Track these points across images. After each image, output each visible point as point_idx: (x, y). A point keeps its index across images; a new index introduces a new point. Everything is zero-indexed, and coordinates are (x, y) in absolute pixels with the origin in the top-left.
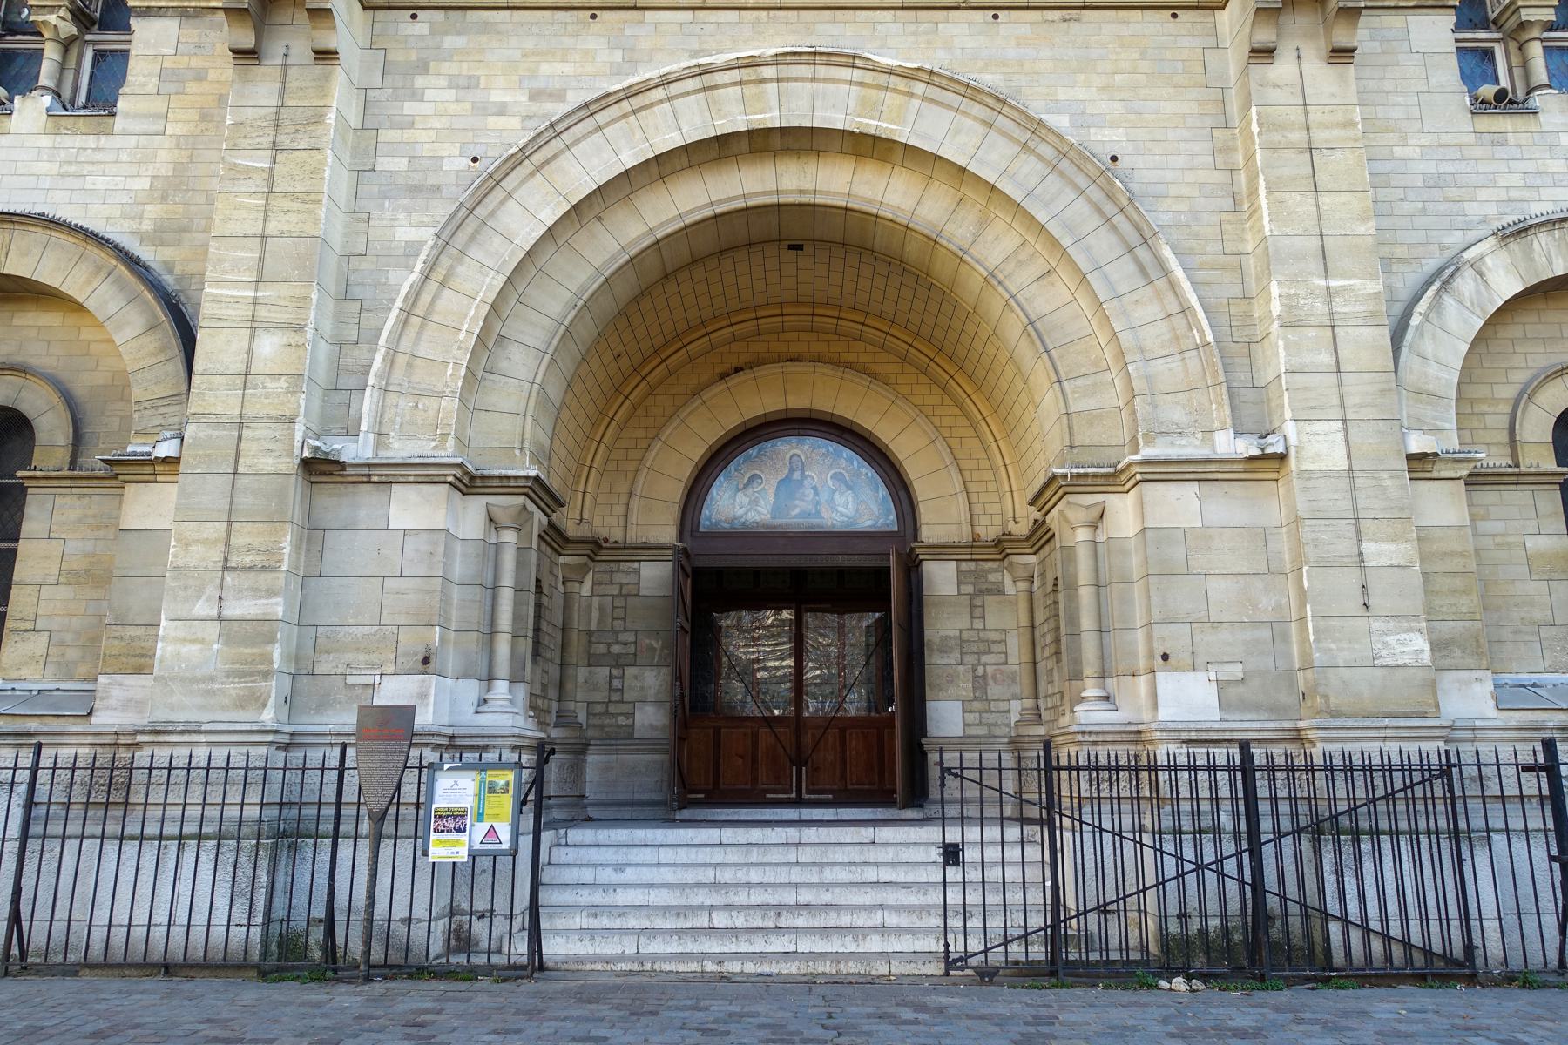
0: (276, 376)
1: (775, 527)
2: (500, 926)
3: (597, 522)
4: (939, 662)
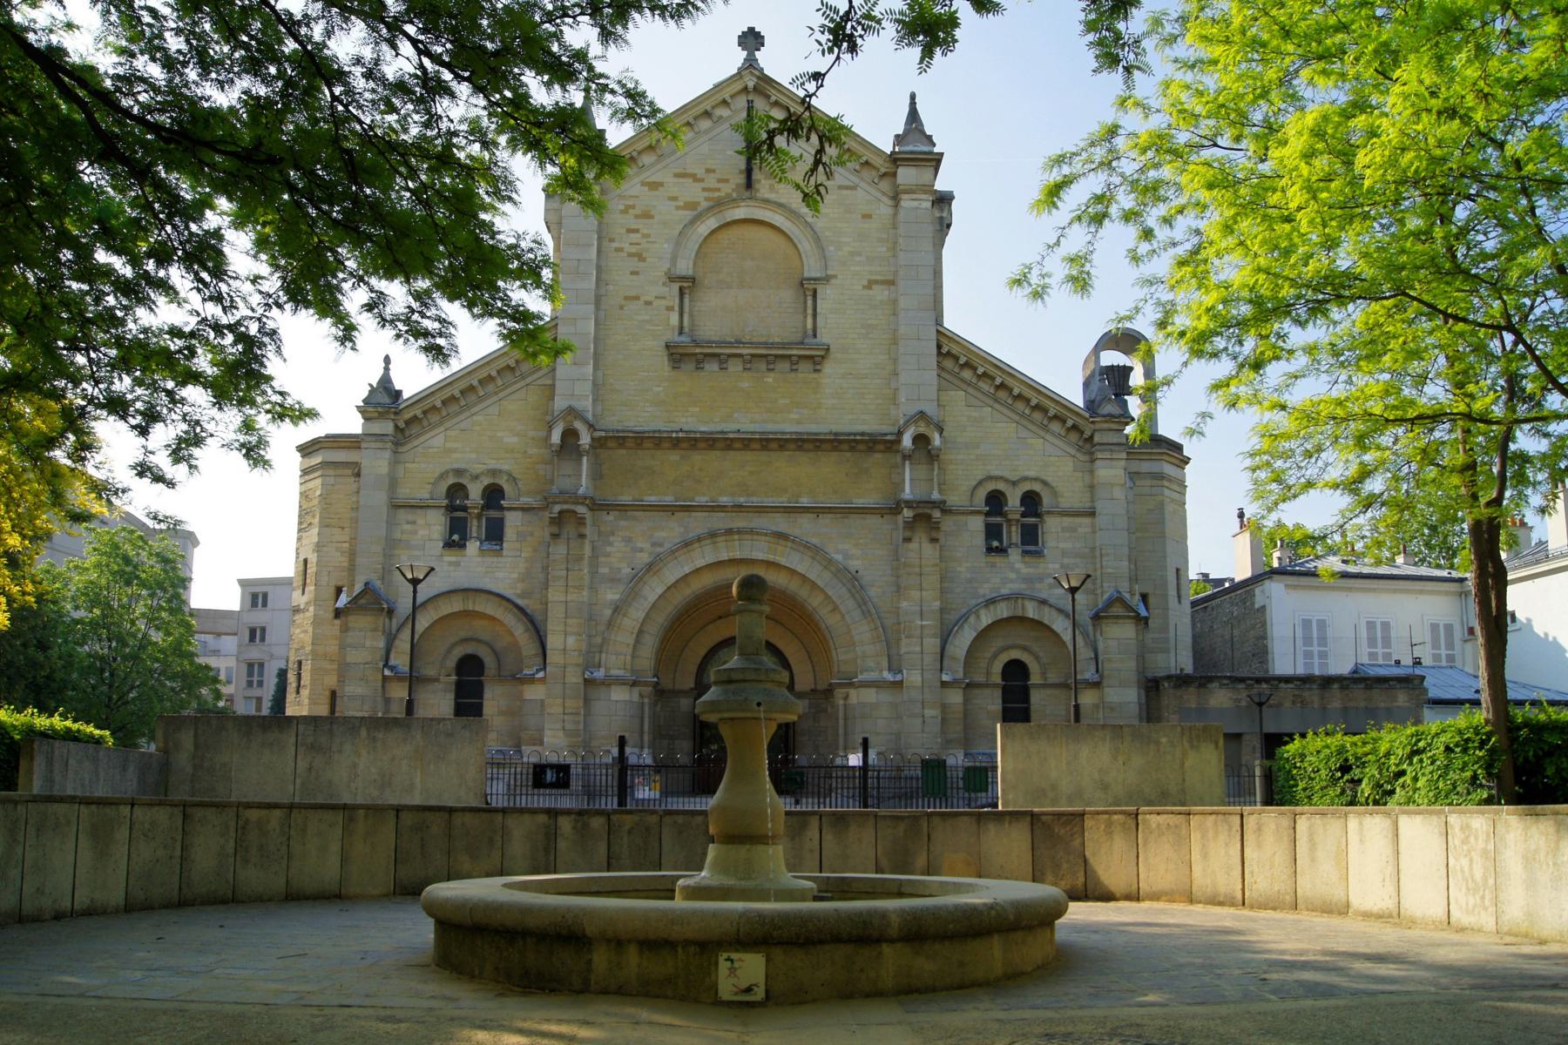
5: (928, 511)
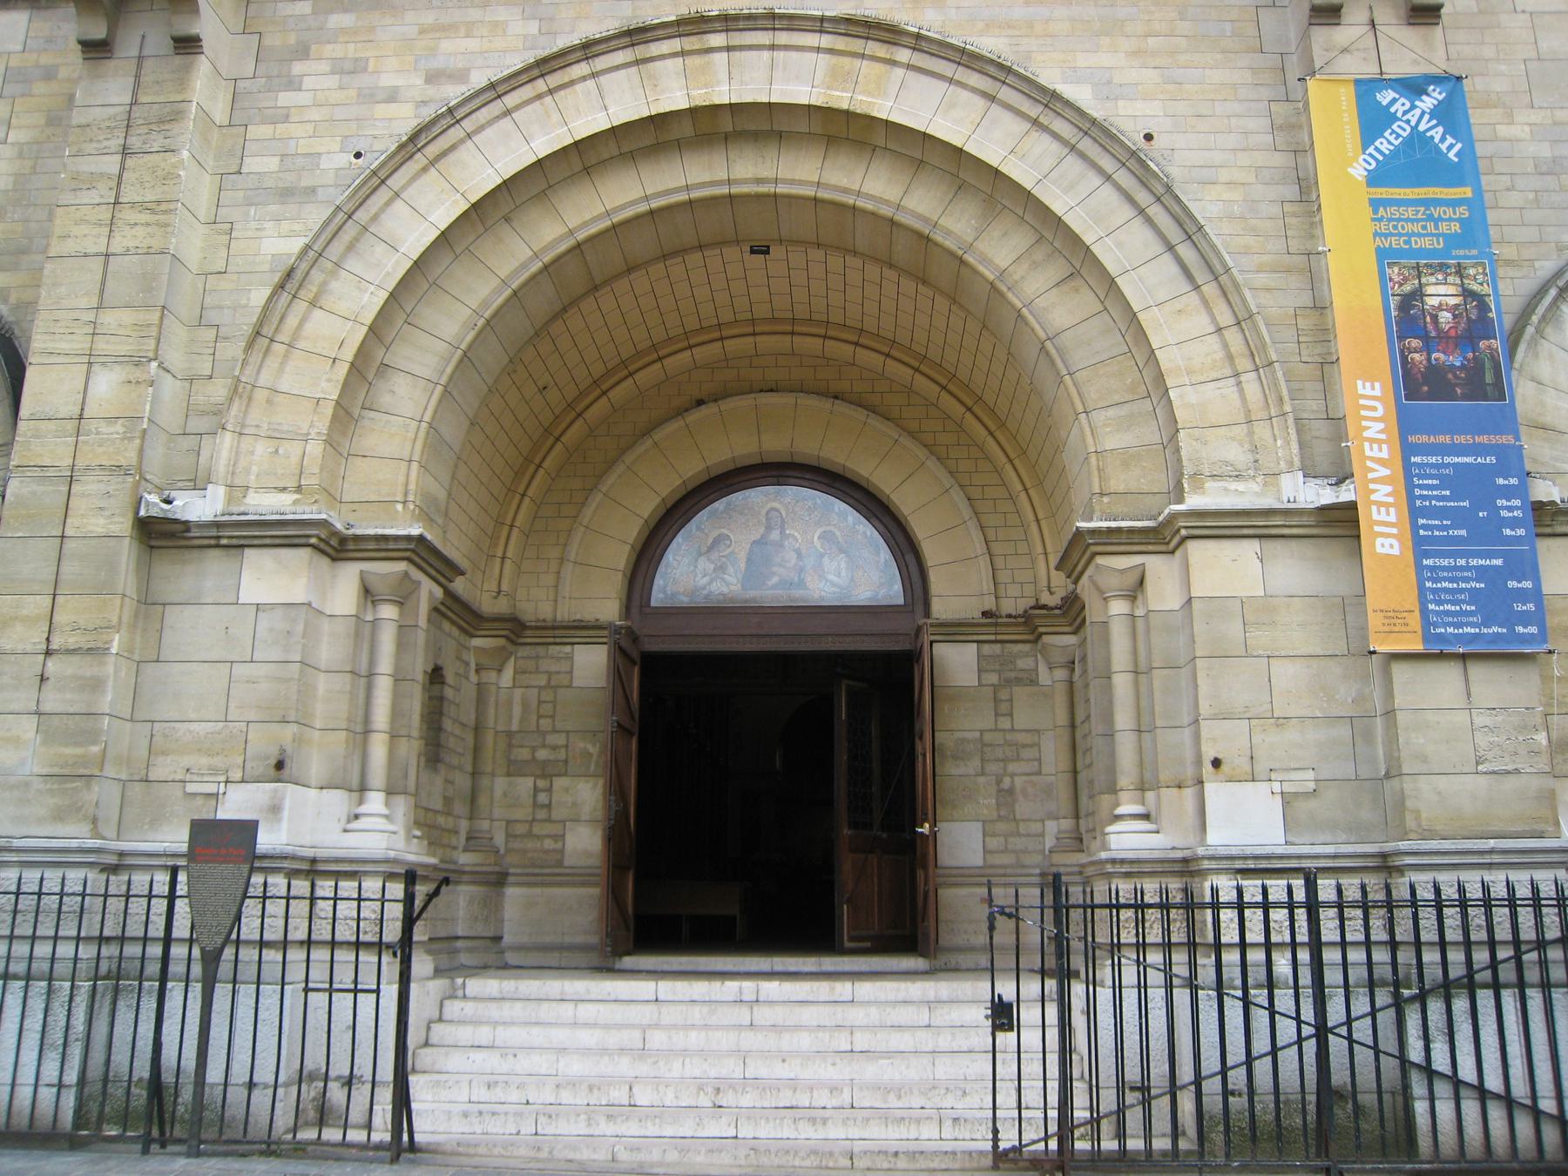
1: (747, 601)
2: (361, 1095)
3: (521, 594)
4: (954, 771)
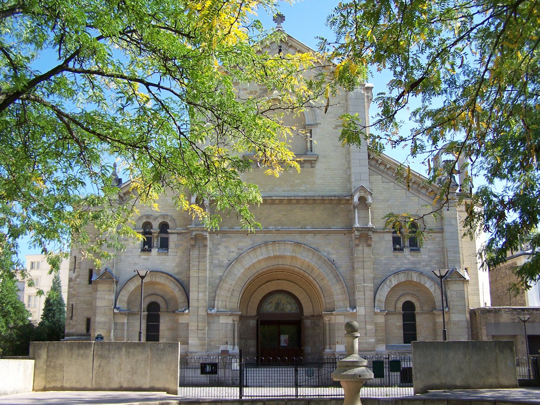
0: (202, 300)
5: (367, 232)
